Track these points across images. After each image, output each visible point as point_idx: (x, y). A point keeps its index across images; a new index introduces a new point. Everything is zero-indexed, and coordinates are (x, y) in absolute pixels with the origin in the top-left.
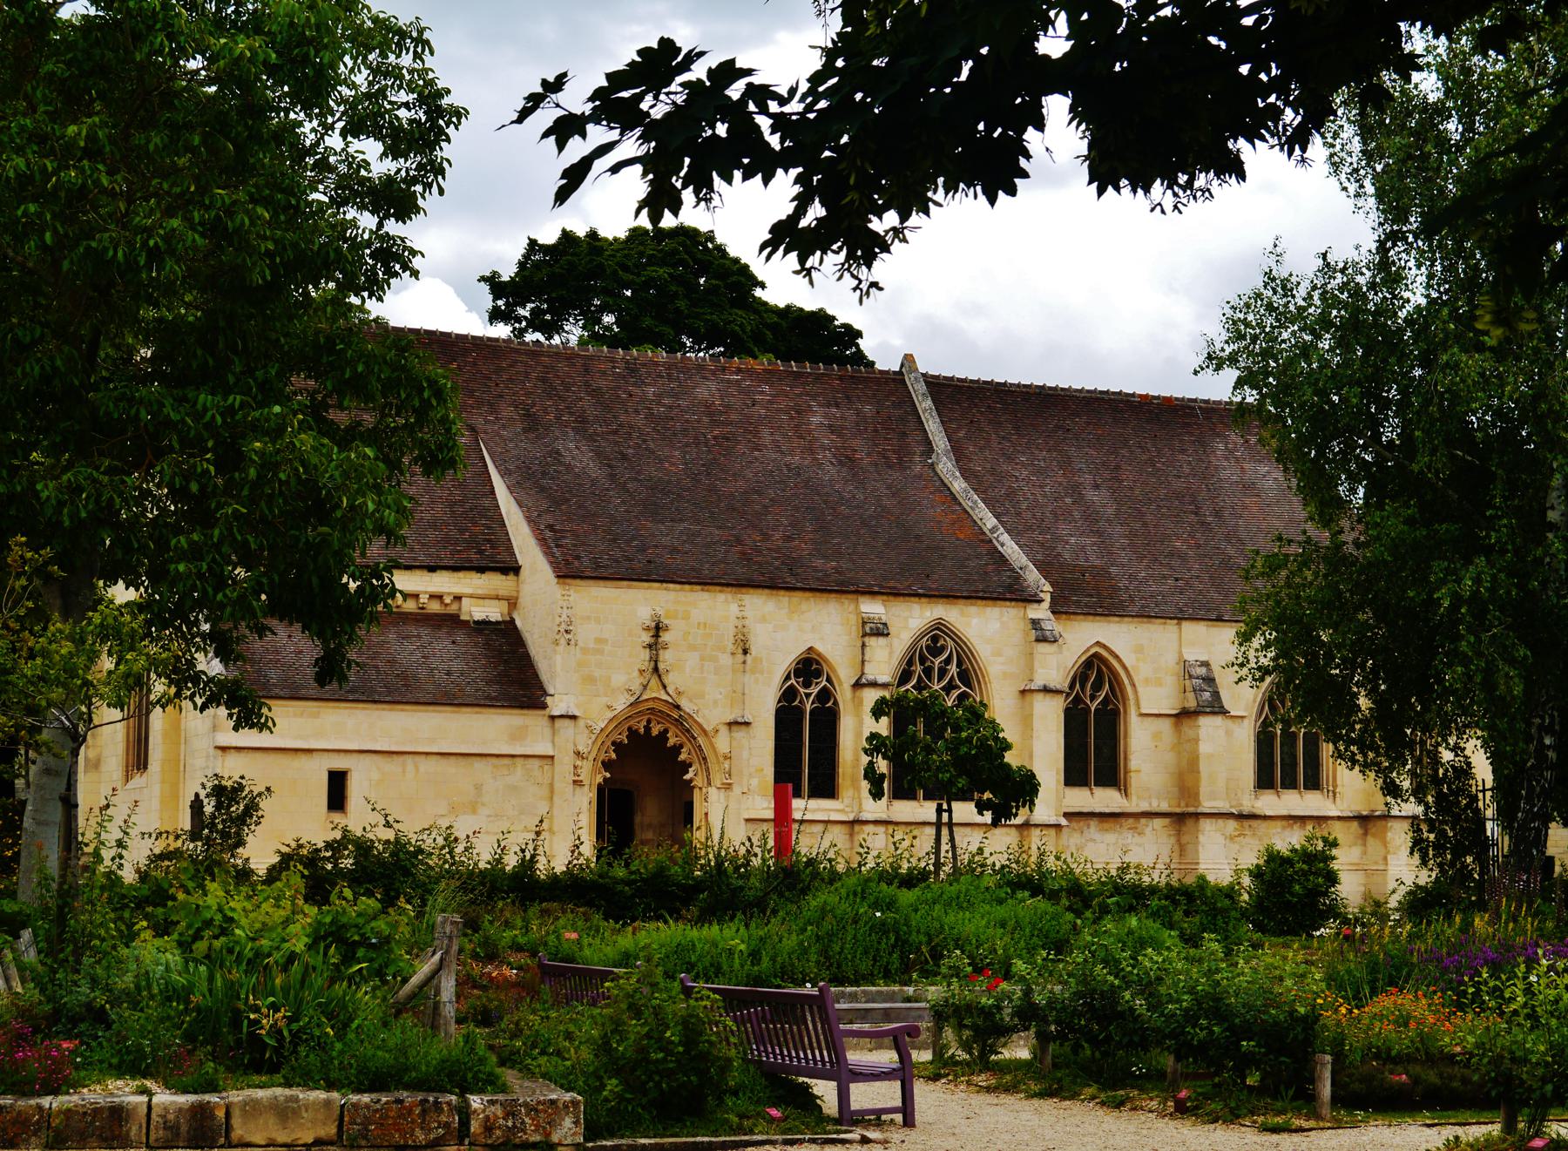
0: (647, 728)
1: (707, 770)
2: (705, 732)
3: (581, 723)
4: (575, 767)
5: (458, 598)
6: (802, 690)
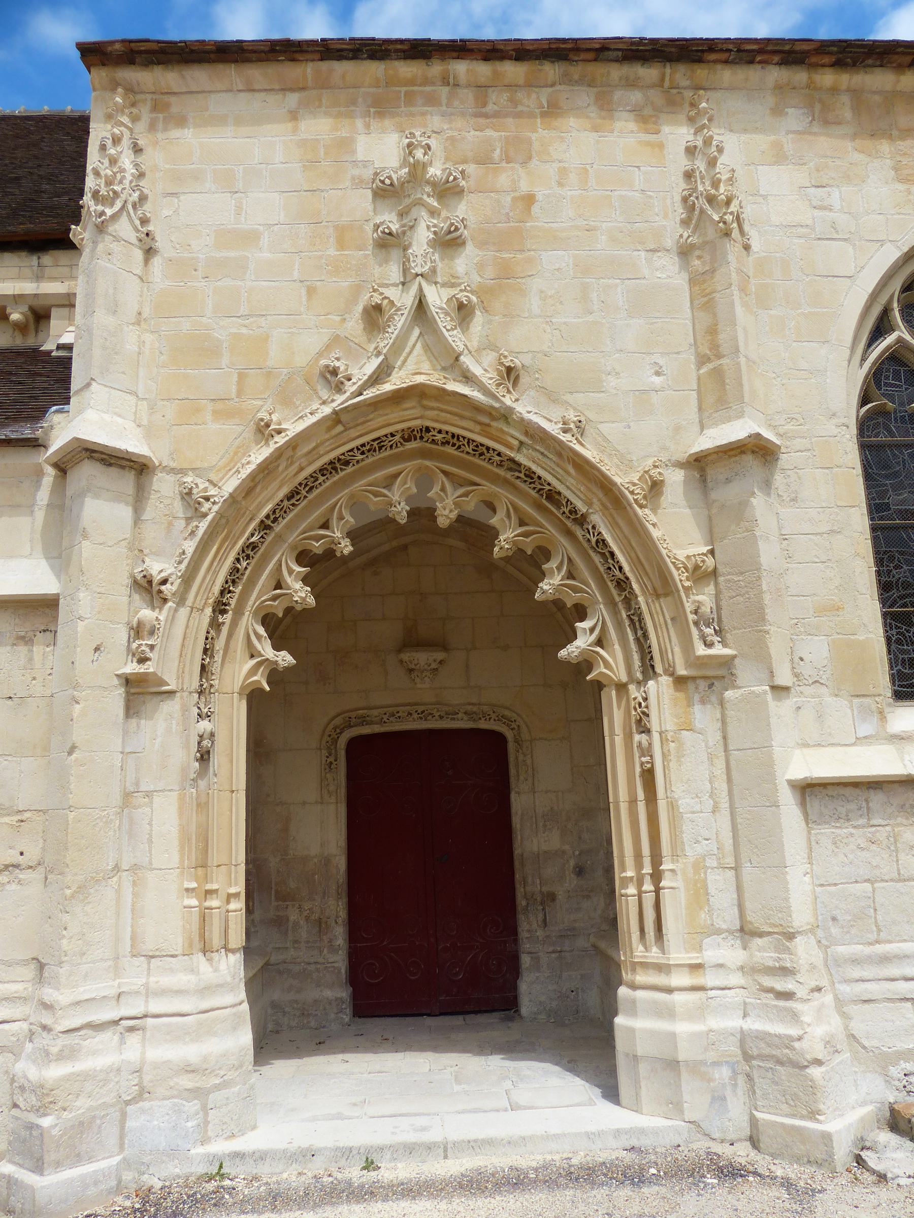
1: (637, 621)
2: (606, 486)
4: (138, 630)
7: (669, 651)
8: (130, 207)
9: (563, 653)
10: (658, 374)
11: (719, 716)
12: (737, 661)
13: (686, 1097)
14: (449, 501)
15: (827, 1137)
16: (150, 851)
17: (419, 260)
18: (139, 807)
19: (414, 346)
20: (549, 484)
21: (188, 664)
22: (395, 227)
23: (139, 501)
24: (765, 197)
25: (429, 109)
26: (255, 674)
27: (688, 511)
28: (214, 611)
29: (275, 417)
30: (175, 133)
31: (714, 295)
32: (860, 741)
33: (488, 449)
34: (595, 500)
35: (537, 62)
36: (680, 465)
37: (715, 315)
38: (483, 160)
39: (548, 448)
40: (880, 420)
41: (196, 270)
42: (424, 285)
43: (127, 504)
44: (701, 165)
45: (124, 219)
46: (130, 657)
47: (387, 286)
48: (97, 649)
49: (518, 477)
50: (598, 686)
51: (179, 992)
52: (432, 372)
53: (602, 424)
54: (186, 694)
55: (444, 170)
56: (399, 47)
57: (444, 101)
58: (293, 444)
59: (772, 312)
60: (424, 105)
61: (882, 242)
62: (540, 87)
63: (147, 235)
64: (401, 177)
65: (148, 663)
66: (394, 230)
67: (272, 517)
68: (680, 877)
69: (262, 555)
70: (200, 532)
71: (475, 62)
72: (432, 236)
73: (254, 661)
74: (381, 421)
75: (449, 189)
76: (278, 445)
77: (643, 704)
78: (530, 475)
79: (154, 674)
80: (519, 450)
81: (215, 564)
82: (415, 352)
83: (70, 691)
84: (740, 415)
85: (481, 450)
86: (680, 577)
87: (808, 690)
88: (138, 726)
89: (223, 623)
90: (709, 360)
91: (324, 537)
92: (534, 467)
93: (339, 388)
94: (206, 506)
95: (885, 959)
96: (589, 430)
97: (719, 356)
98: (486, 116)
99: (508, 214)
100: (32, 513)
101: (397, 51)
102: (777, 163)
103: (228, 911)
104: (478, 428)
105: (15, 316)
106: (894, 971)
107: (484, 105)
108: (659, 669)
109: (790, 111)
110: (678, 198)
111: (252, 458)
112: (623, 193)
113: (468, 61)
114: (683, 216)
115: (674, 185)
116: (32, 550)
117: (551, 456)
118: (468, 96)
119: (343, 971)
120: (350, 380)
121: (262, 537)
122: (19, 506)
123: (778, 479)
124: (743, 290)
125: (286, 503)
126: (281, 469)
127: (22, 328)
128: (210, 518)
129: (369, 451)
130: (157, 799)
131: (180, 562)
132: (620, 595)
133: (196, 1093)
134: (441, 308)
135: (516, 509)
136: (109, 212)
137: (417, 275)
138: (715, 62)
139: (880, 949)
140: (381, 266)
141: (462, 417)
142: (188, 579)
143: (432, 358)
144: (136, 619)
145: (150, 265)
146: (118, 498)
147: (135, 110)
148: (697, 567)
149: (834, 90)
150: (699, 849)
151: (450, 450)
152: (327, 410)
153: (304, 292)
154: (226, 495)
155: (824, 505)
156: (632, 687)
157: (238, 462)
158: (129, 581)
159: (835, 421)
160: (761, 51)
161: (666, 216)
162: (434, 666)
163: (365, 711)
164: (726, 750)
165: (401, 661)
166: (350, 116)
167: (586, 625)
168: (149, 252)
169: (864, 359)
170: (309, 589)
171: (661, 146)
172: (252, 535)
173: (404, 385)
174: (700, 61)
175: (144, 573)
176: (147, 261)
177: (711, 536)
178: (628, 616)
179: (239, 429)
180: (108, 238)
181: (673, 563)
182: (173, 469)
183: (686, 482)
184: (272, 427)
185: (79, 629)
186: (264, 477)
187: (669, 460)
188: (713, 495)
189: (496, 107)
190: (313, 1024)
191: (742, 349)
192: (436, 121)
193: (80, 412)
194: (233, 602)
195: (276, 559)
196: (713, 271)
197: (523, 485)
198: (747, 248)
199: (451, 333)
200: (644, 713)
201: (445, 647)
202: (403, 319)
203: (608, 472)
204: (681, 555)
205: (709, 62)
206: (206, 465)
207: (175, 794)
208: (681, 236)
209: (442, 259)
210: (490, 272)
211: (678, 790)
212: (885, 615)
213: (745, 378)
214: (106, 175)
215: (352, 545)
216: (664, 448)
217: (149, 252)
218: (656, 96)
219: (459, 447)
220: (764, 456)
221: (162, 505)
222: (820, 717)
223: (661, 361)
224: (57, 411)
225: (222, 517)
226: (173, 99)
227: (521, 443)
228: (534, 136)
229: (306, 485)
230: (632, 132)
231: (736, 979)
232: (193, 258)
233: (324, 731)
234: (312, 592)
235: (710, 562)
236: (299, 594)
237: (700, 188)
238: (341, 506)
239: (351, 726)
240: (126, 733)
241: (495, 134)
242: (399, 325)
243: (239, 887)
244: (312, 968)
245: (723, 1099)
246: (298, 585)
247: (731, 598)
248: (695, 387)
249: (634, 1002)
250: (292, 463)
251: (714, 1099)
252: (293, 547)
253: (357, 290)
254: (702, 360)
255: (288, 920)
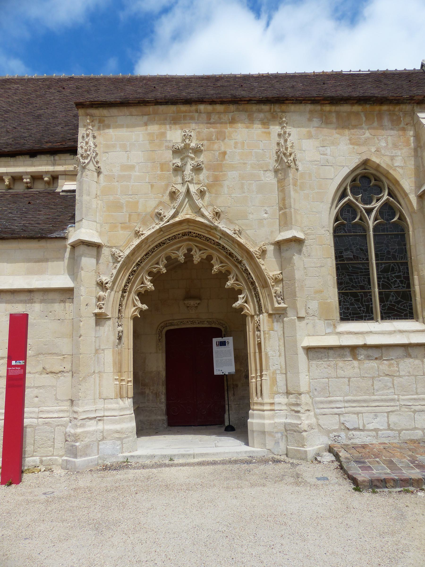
0: (189, 256)
1: (257, 295)
2: (248, 252)
3: (105, 252)
4: (99, 299)
5: (55, 178)
6: (360, 205)
7: (267, 305)
8: (93, 159)
9: (234, 305)
10: (266, 213)
11: (282, 326)
12: (288, 309)
13: (267, 442)
14: (197, 256)
15: (306, 452)
16: (104, 367)
17: (188, 176)
18: (100, 354)
19: (186, 205)
20: (230, 251)
21: (114, 309)
22: (179, 164)
23: (98, 257)
24: (304, 151)
25: (192, 121)
26: (135, 312)
27: (274, 259)
28: (122, 292)
29: (141, 230)
30: (107, 131)
31: (285, 187)
32: (326, 334)
33: (210, 239)
34: (244, 256)
35: (228, 104)
36: (272, 244)
37: (285, 194)
38: (209, 139)
39: (229, 239)
40: (342, 227)
41: (114, 179)
42: (189, 184)
43: (94, 258)
44: (282, 142)
45: (91, 163)
46: (96, 307)
47: (177, 184)
48: (87, 305)
49: (220, 248)
50: (245, 316)
51: (114, 410)
52: (192, 214)
53: (247, 231)
54: (114, 319)
55: (196, 144)
56: (181, 101)
57: (196, 118)
58: (147, 238)
59: (305, 192)
60: (189, 120)
61: (343, 166)
62: (229, 113)
63: (98, 167)
64: (182, 147)
65: (102, 309)
66: (179, 166)
67: (140, 262)
68: (268, 376)
69: (137, 273)
70: (118, 267)
71: (207, 105)
72: (192, 167)
73: (135, 308)
74: (175, 230)
75: (198, 150)
76: (142, 239)
77: (259, 322)
78: (223, 247)
79: (104, 312)
80: (220, 239)
81: (123, 277)
82: (186, 207)
83: (79, 318)
84: (291, 229)
85: (208, 239)
86: (270, 282)
87: (311, 318)
88: (99, 328)
89: (125, 296)
90: (282, 209)
91: (157, 267)
92: (225, 245)
93: (162, 220)
94: (120, 259)
95: (331, 402)
96: (243, 233)
97: (286, 208)
98: (211, 124)
99: (217, 158)
100: (63, 260)
101: (180, 102)
102: (309, 138)
103: (128, 386)
104: (206, 232)
105: (46, 179)
106: (333, 405)
107: (210, 119)
108: (264, 311)
109: (314, 119)
110: (275, 152)
111: (134, 243)
112: (256, 150)
113: (204, 105)
114: (276, 159)
115: (273, 147)
116: (64, 272)
117: (230, 242)
118: (204, 116)
119: (164, 410)
120: (165, 217)
121: (137, 268)
122: (59, 258)
123: (304, 249)
124: (295, 185)
125: (145, 257)
126: (143, 246)
127: (48, 183)
128: (121, 263)
129: (171, 239)
130: (106, 351)
131: (111, 277)
132: (252, 287)
133: (119, 439)
134: (195, 193)
135: (219, 258)
136: (86, 161)
137: (187, 181)
138: (289, 103)
139: (329, 399)
140: (175, 177)
141: (202, 229)
142: (114, 282)
143: (192, 209)
144: (98, 295)
145: (99, 177)
146: (92, 257)
147: (93, 123)
148: (276, 278)
149: (330, 112)
150: (274, 368)
151: (198, 239)
152: (158, 227)
153: (150, 186)
154: (126, 255)
155: (319, 257)
156: (255, 317)
157: (129, 244)
158: (96, 283)
159: (324, 229)
160: (304, 100)
161: (270, 159)
162: (196, 305)
163: (172, 321)
164: (284, 337)
165: (184, 304)
166: (165, 124)
167: (241, 296)
168: (99, 173)
169: (336, 206)
170: (152, 284)
171: (269, 133)
172: (134, 268)
173: (182, 219)
174: (283, 103)
175: (100, 280)
176: (98, 176)
177: (282, 268)
178: (255, 294)
179: (130, 233)
180: (86, 170)
181: (268, 277)
182: (108, 246)
183: (274, 250)
184: (140, 233)
185: (81, 299)
186: (138, 249)
187: (269, 243)
188: (282, 255)
189: (214, 120)
190: (154, 427)
191: (292, 206)
192: (193, 126)
193: (79, 228)
194: (128, 289)
195: (142, 275)
196: (285, 179)
197: (221, 251)
198: (297, 170)
199: (198, 201)
200: (259, 325)
201: (200, 298)
202: (182, 196)
203: (248, 247)
204: (271, 274)
205: (286, 103)
206: (119, 245)
207: (111, 350)
208: (275, 166)
209: (195, 175)
210: (211, 179)
211: (268, 349)
212: (339, 293)
213: (293, 216)
214: (85, 149)
215: (166, 270)
216: (267, 239)
217: (99, 173)
218: (268, 115)
219: (201, 238)
220: (299, 242)
221: (105, 258)
222: (314, 326)
223: (267, 209)
224: (71, 227)
225: (125, 262)
226: (106, 119)
227: (221, 237)
228: (226, 130)
229: (151, 251)
230: (260, 128)
231: (284, 407)
232: (113, 175)
233: (157, 328)
234: (153, 286)
235: (281, 277)
236: (149, 286)
237: (281, 150)
238: (162, 258)
239: (167, 326)
240: (96, 331)
241: (213, 130)
242: (181, 199)
243: (131, 379)
244: (154, 409)
245: (279, 443)
246: (149, 283)
247: (287, 288)
248: (278, 218)
249: (253, 414)
250: (146, 245)
251: (275, 443)
252: (147, 271)
253: (167, 186)
254: (280, 209)
255: (145, 393)
